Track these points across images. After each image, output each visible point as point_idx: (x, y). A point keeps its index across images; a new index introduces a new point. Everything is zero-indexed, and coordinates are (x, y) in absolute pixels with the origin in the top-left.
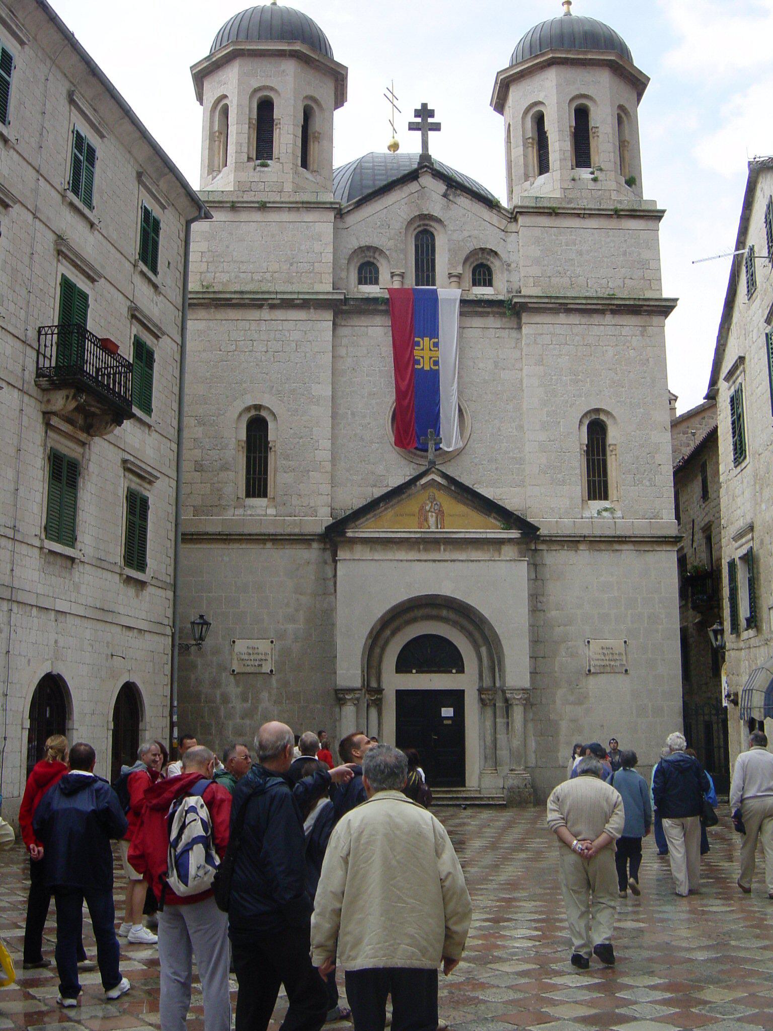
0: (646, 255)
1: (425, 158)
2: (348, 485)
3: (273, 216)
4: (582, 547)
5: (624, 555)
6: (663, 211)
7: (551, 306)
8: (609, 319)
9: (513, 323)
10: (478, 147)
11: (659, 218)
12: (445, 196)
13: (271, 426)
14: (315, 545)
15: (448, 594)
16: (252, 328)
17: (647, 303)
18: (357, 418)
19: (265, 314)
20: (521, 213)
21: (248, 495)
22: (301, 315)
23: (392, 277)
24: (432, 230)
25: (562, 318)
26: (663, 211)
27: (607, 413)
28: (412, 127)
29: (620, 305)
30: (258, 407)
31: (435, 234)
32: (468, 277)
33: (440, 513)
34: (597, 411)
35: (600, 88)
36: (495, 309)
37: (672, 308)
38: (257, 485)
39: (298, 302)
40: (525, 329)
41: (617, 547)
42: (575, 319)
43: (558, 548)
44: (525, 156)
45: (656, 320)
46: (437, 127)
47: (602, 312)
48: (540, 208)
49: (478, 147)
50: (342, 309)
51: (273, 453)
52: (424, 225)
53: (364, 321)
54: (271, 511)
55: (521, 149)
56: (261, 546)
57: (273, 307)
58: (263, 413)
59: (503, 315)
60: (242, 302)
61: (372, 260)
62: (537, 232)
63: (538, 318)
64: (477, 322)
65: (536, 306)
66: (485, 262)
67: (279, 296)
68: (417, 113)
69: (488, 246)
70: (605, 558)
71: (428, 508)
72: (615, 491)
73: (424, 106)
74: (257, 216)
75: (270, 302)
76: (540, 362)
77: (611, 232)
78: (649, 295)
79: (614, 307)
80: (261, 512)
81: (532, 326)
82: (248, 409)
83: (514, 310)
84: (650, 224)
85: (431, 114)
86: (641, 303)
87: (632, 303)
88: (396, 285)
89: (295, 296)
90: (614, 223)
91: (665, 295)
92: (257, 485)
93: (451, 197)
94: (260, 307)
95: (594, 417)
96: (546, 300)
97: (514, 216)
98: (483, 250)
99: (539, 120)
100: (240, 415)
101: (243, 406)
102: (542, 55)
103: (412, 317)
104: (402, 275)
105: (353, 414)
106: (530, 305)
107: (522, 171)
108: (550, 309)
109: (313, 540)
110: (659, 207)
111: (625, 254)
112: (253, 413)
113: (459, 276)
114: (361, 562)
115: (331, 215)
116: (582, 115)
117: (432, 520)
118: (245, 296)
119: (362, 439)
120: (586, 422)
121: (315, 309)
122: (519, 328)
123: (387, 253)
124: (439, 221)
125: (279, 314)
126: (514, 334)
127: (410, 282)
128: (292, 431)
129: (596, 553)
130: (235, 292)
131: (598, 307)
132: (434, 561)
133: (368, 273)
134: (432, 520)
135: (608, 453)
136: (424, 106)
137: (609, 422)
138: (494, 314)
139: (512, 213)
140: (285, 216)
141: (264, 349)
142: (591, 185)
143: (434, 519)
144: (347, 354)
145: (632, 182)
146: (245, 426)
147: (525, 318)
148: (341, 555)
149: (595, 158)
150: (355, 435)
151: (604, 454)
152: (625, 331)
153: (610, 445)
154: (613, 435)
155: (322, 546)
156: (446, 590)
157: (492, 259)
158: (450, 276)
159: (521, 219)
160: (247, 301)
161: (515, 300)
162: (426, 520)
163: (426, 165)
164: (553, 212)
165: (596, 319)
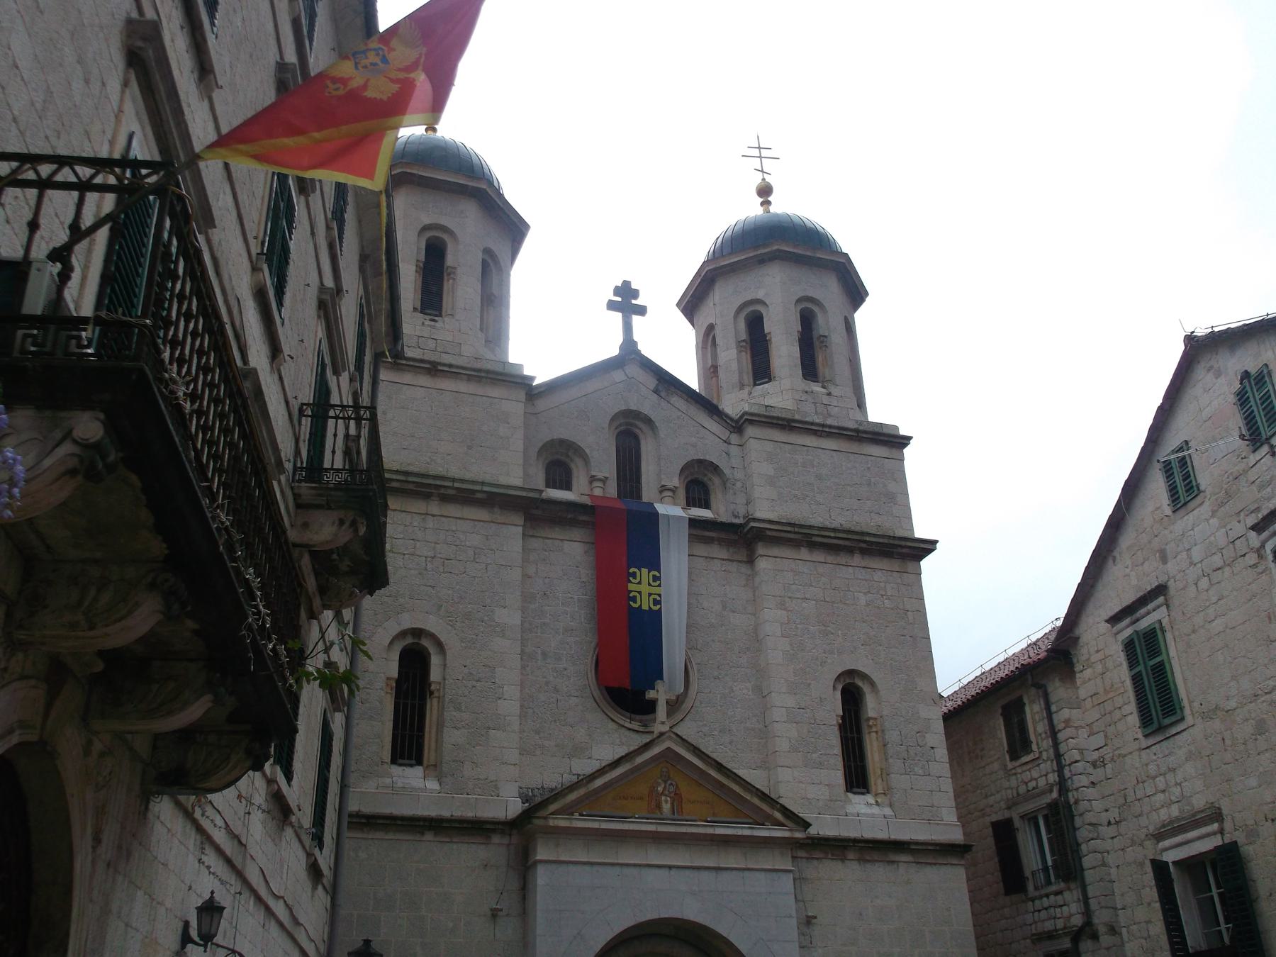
0: (892, 487)
1: (629, 346)
2: (538, 752)
3: (446, 384)
4: (851, 855)
5: (902, 867)
6: (910, 438)
7: (792, 536)
8: (857, 559)
9: (743, 555)
10: (675, 348)
11: (905, 445)
12: (656, 391)
13: (435, 660)
14: (496, 839)
15: (692, 918)
16: (416, 524)
17: (903, 543)
18: (549, 661)
19: (434, 507)
20: (751, 422)
21: (394, 761)
22: (482, 514)
23: (591, 483)
24: (637, 431)
25: (804, 553)
26: (910, 438)
27: (864, 677)
28: (612, 306)
29: (872, 543)
30: (418, 633)
31: (641, 436)
32: (682, 494)
33: (677, 799)
34: (851, 673)
35: (828, 291)
36: (723, 536)
37: (930, 551)
38: (409, 744)
39: (479, 496)
40: (762, 564)
41: (893, 857)
42: (819, 556)
43: (822, 855)
44: (739, 362)
45: (910, 566)
46: (642, 311)
47: (850, 550)
48: (773, 417)
49: (675, 348)
50: (535, 513)
51: (435, 701)
52: (627, 424)
53: (557, 533)
54: (432, 785)
55: (733, 353)
56: (418, 837)
57: (445, 499)
58: (425, 642)
59: (729, 544)
60: (406, 486)
61: (563, 458)
62: (769, 447)
63: (775, 551)
64: (701, 549)
65: (774, 534)
66: (700, 477)
67: (456, 485)
68: (617, 291)
69: (707, 458)
70: (879, 872)
71: (660, 789)
72: (879, 781)
73: (626, 284)
74: (424, 380)
75: (442, 491)
76: (782, 606)
77: (852, 457)
78: (900, 533)
79: (864, 545)
80: (415, 790)
81: (769, 562)
82: (403, 634)
83: (744, 539)
84: (894, 453)
85: (635, 294)
86: (896, 542)
87: (886, 541)
88: (598, 492)
89: (478, 488)
90: (854, 447)
91: (920, 533)
92: (409, 744)
93: (663, 394)
94: (427, 496)
95: (848, 681)
96: (789, 529)
97: (738, 426)
98: (700, 462)
99: (755, 324)
100: (391, 643)
101: (396, 630)
102: (765, 246)
103: (624, 536)
104: (604, 480)
105: (544, 654)
106: (769, 533)
107: (735, 378)
108: (790, 540)
109: (494, 831)
110: (902, 432)
111: (869, 484)
112: (409, 640)
113: (674, 490)
114: (571, 867)
115: (522, 395)
116: (807, 320)
117: (666, 807)
118: (410, 479)
119: (556, 690)
120: (840, 687)
121: (501, 508)
122: (751, 561)
123: (587, 451)
124: (649, 421)
125: (453, 510)
126: (745, 569)
127: (612, 491)
128: (466, 670)
129: (868, 865)
130: (397, 472)
131: (847, 543)
132: (670, 867)
133: (559, 473)
134: (666, 807)
135: (865, 730)
136: (626, 284)
137: (866, 688)
138: (721, 542)
139: (737, 422)
140: (462, 386)
141: (430, 554)
142: (826, 400)
143: (669, 806)
144: (536, 573)
145: (861, 404)
146: (397, 658)
147: (761, 549)
148: (542, 853)
149: (822, 370)
150: (547, 683)
151: (859, 731)
152: (878, 576)
153: (869, 719)
154: (871, 706)
155: (506, 841)
156: (692, 911)
157: (710, 475)
158: (663, 489)
159: (751, 431)
160: (411, 487)
161: (753, 524)
162: (659, 807)
163: (630, 353)
164: (786, 424)
165: (843, 559)
